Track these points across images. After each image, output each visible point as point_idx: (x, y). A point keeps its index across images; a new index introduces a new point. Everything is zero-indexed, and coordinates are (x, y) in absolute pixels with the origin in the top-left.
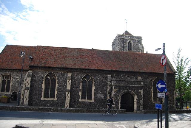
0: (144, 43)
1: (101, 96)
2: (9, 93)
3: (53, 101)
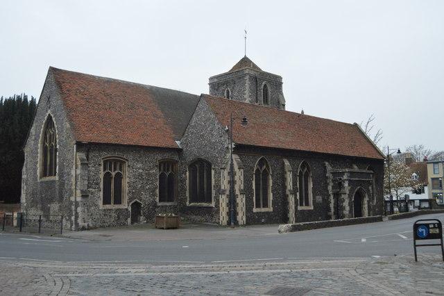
0: (286, 90)
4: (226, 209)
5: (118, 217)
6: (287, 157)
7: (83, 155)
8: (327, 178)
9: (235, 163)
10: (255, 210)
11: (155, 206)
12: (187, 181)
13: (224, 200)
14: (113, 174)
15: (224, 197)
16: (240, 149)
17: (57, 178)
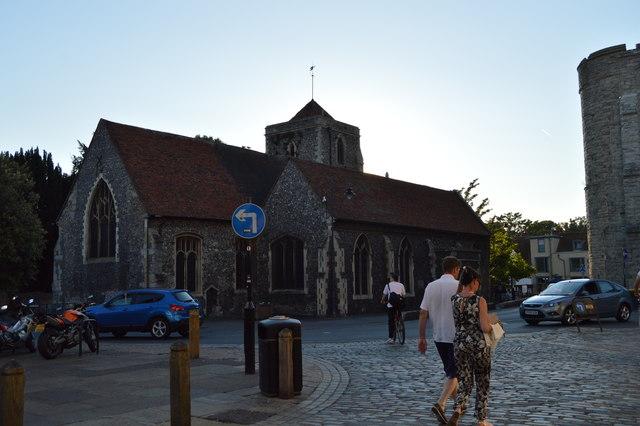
4: (325, 296)
7: (153, 231)
9: (335, 241)
10: (354, 297)
12: (270, 263)
13: (322, 287)
14: (187, 254)
15: (323, 281)
17: (117, 260)
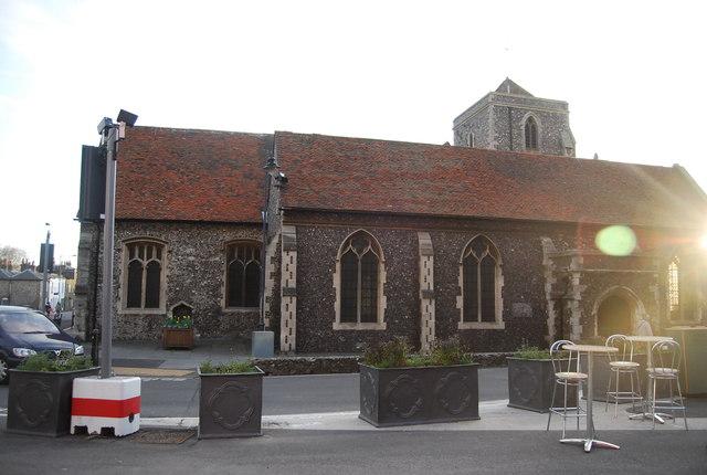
1: (524, 309)
2: (162, 310)
3: (372, 332)
5: (150, 325)
6: (425, 229)
8: (543, 267)
11: (218, 311)
14: (145, 263)
16: (291, 215)
